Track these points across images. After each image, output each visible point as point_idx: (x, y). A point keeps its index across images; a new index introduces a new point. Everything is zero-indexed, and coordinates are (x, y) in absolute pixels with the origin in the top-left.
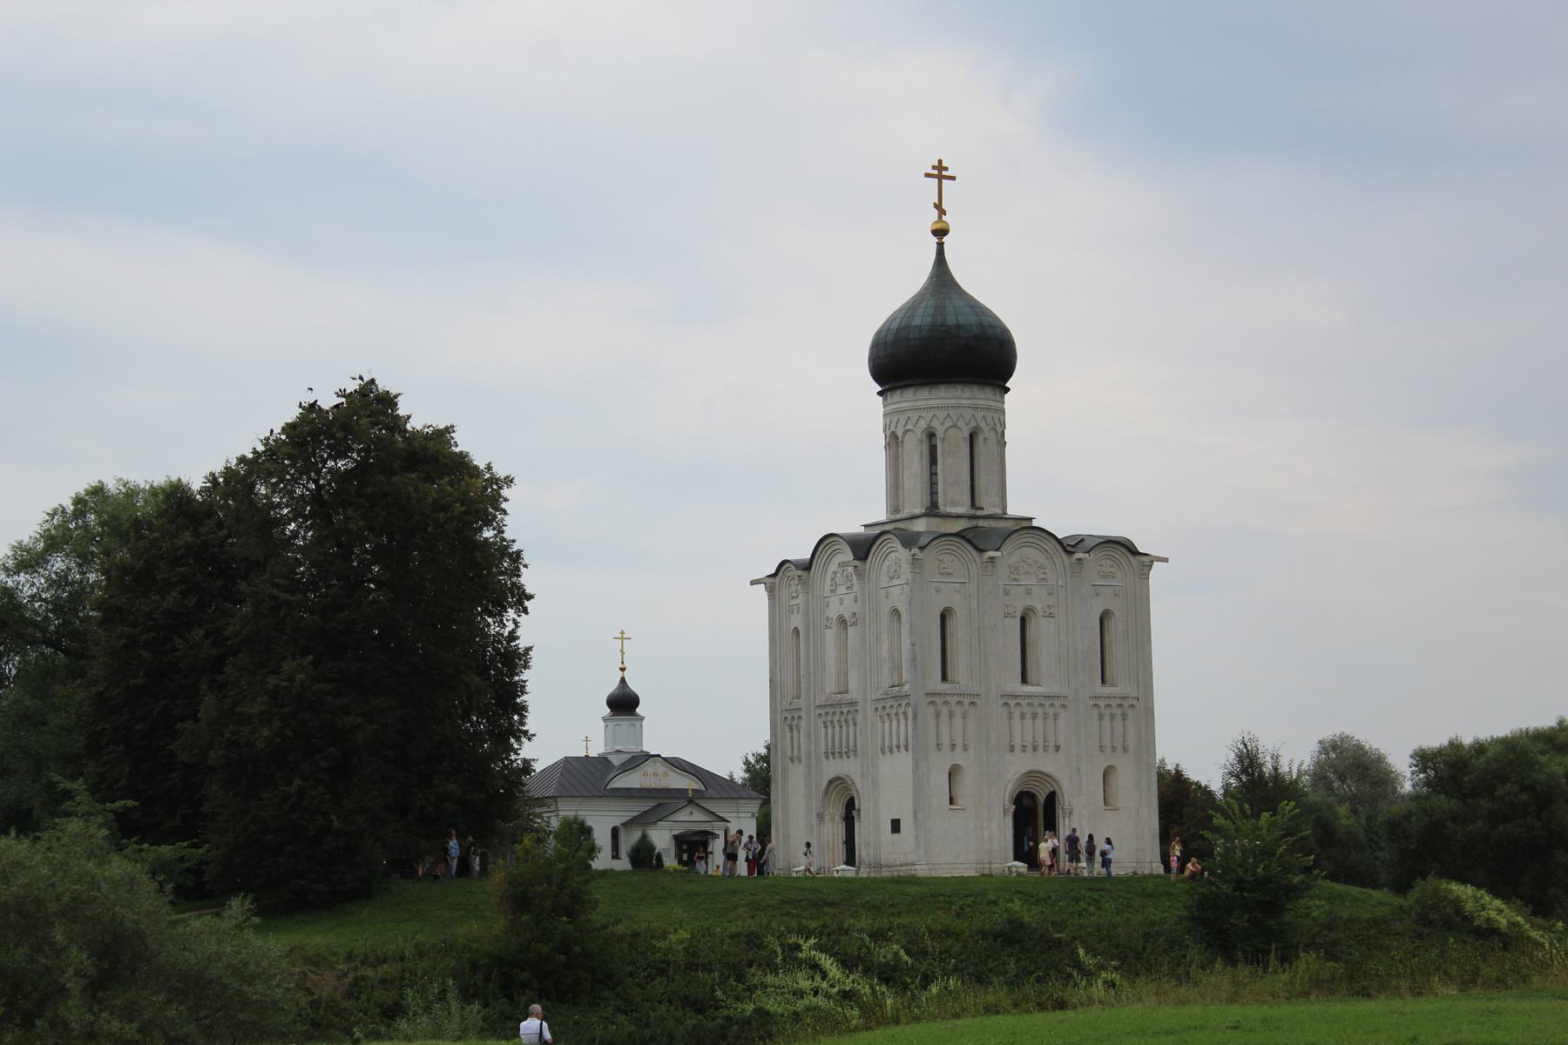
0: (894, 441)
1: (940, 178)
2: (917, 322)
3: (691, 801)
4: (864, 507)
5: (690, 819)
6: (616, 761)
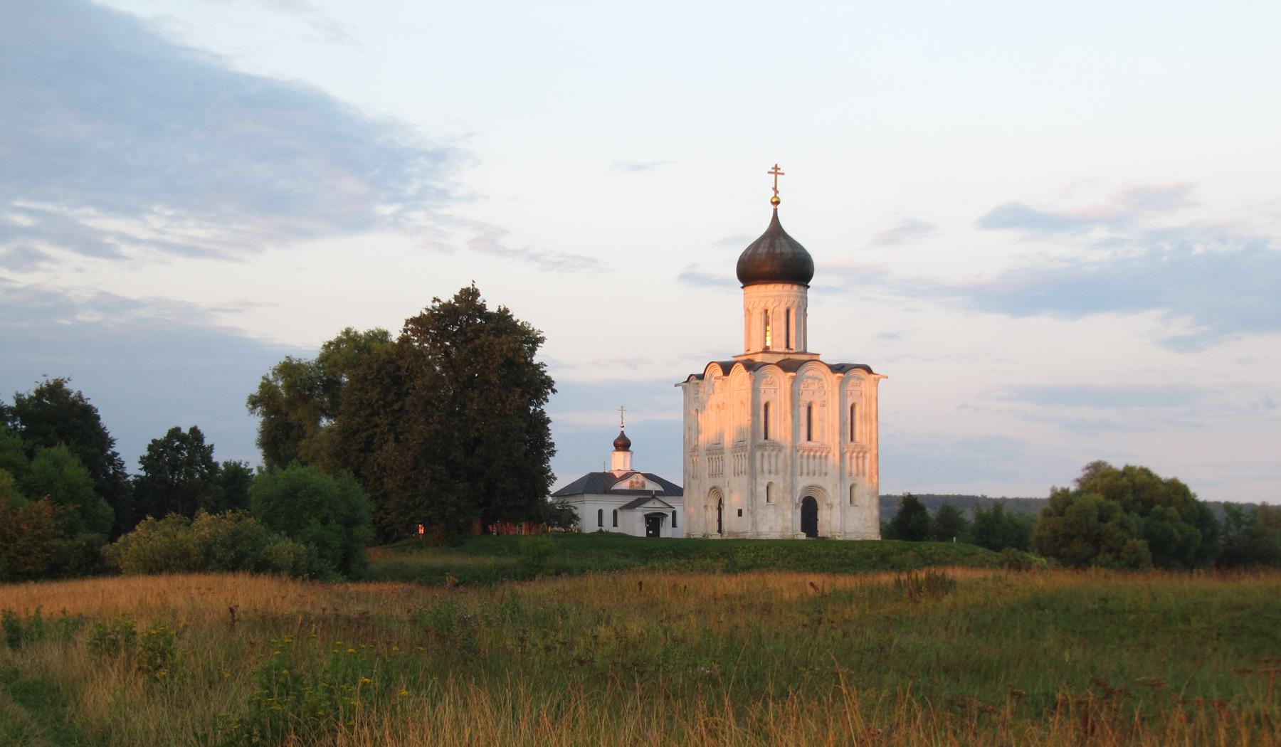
0: (748, 313)
1: (776, 174)
2: (760, 251)
3: (654, 497)
4: (734, 347)
5: (653, 506)
6: (618, 475)
